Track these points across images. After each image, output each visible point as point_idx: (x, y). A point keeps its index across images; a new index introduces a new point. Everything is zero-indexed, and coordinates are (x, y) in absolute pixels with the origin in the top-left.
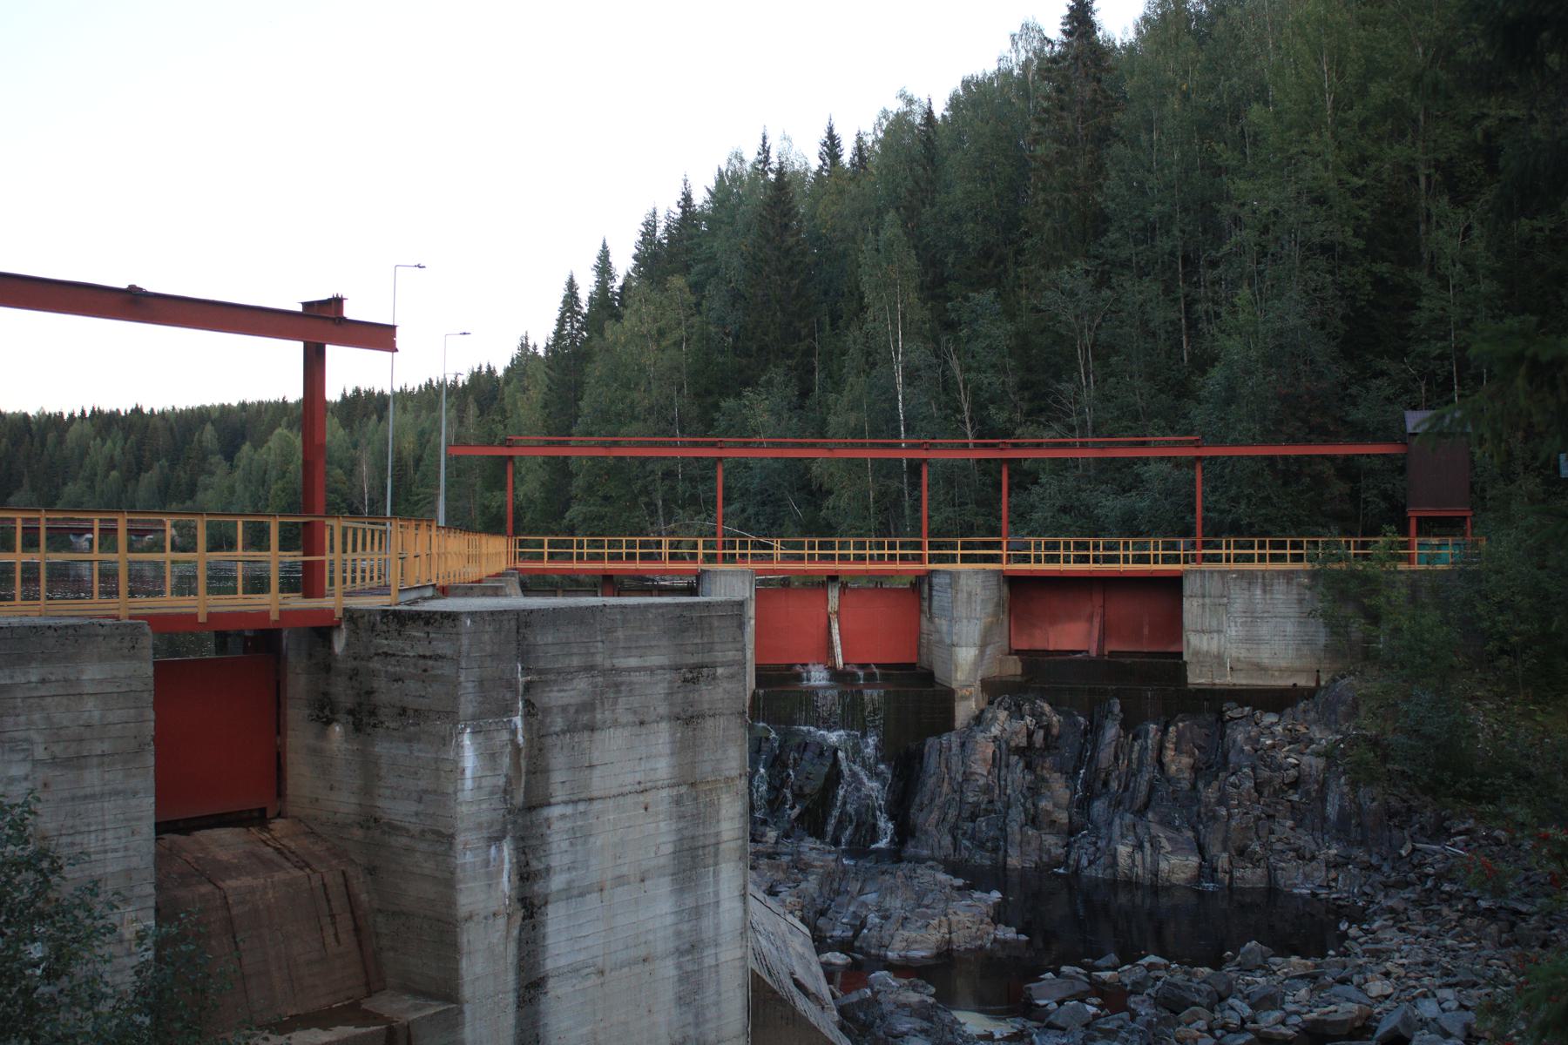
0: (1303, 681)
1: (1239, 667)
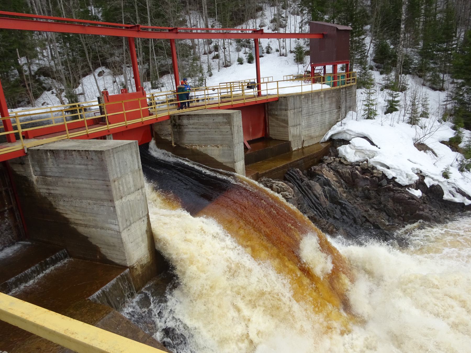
1: (306, 139)
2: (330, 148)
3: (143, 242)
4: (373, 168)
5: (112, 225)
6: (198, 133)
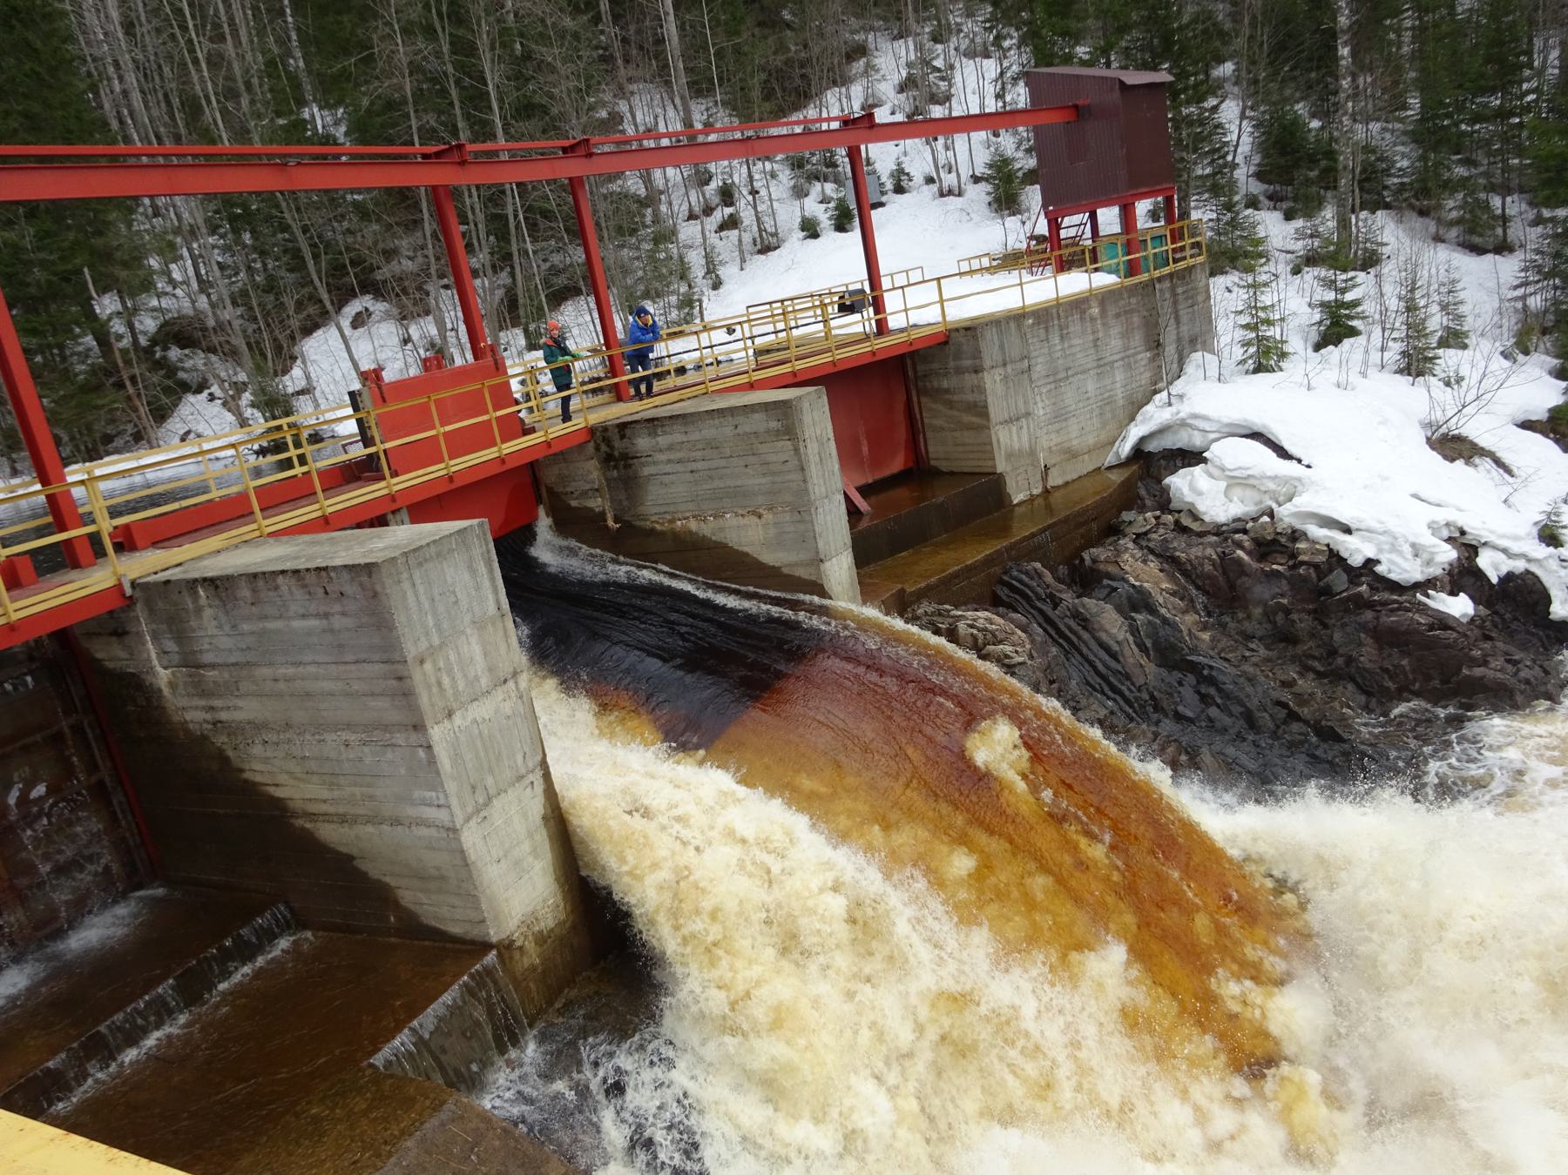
1: (1053, 462)
2: (1139, 484)
3: (536, 858)
4: (1296, 535)
5: (427, 809)
6: (688, 477)
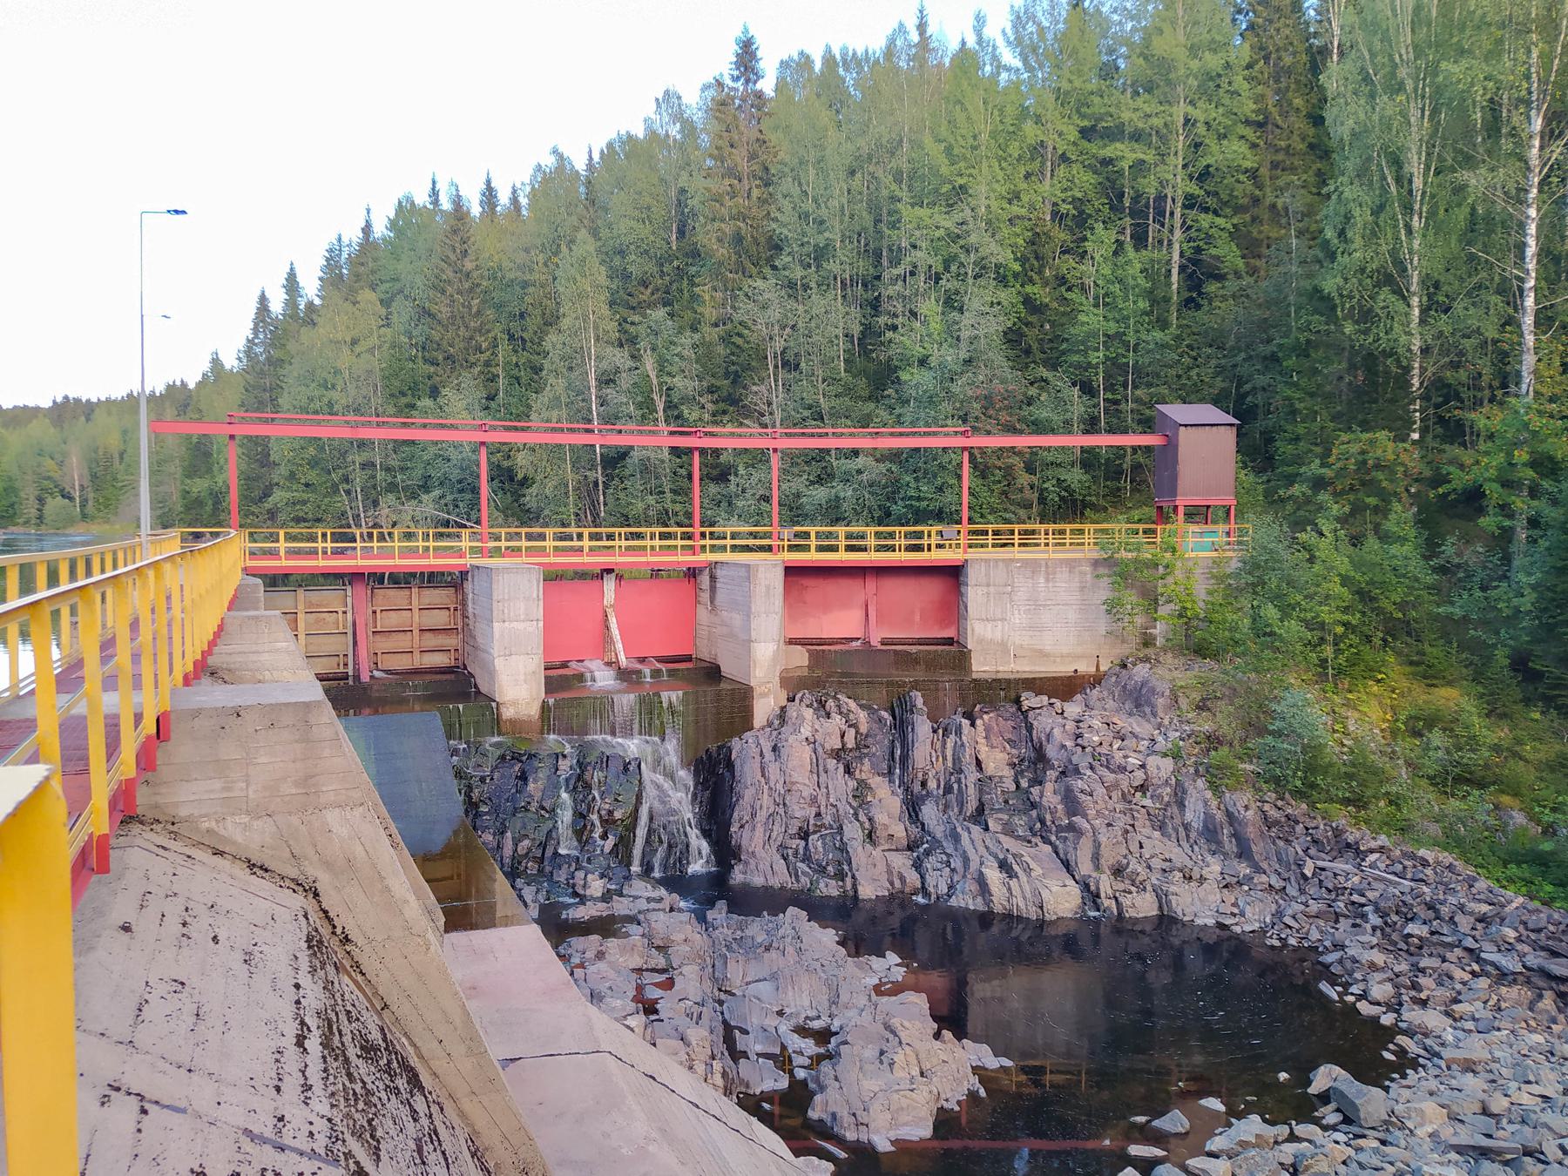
0: (1086, 668)
